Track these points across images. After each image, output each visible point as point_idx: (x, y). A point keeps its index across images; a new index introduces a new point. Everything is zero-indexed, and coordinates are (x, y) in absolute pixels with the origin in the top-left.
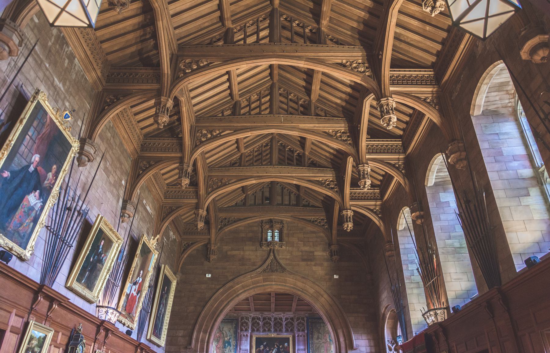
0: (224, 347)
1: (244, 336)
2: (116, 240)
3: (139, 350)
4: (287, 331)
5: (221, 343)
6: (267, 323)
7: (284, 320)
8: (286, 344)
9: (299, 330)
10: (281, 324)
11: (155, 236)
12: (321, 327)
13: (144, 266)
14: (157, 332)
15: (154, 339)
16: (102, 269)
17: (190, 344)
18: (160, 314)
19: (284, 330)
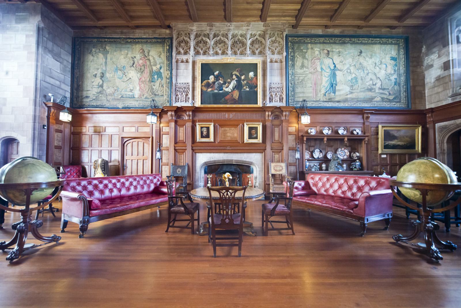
0: (152, 81)
4: (253, 53)
5: (146, 75)
7: (248, 36)
8: (251, 74)
9: (273, 53)
10: (244, 44)
12: (308, 49)
19: (248, 52)
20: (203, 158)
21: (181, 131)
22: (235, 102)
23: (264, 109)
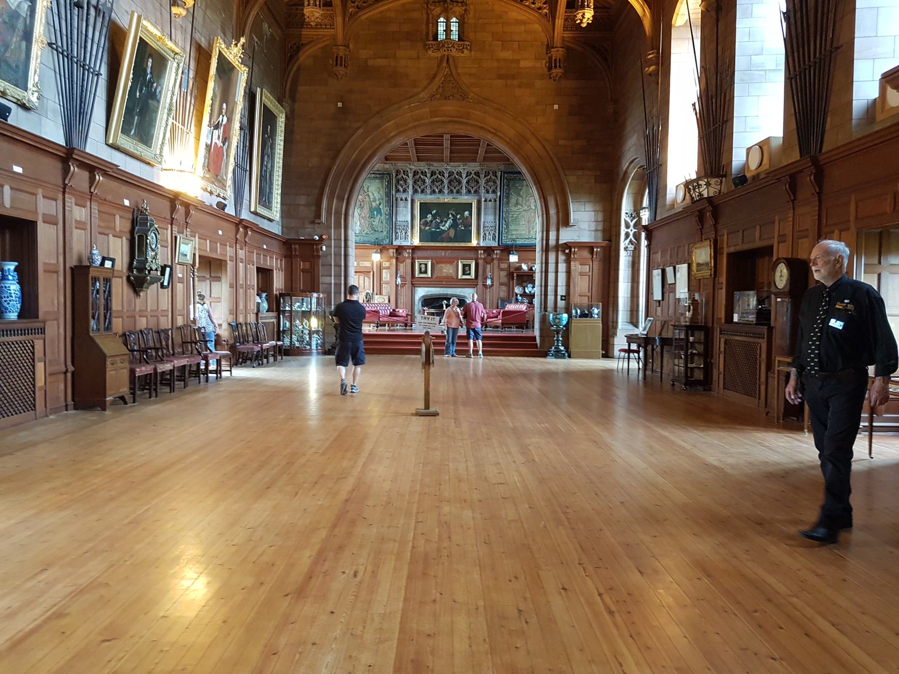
1: (402, 200)
2: (173, 55)
3: (241, 229)
4: (469, 192)
6: (437, 180)
7: (464, 176)
8: (467, 213)
9: (488, 192)
10: (460, 182)
11: (239, 41)
13: (226, 94)
14: (264, 198)
15: (261, 210)
16: (158, 108)
17: (318, 216)
18: (266, 171)
19: (464, 191)
20: (421, 292)
21: (401, 266)
22: (450, 240)
23: (475, 249)
